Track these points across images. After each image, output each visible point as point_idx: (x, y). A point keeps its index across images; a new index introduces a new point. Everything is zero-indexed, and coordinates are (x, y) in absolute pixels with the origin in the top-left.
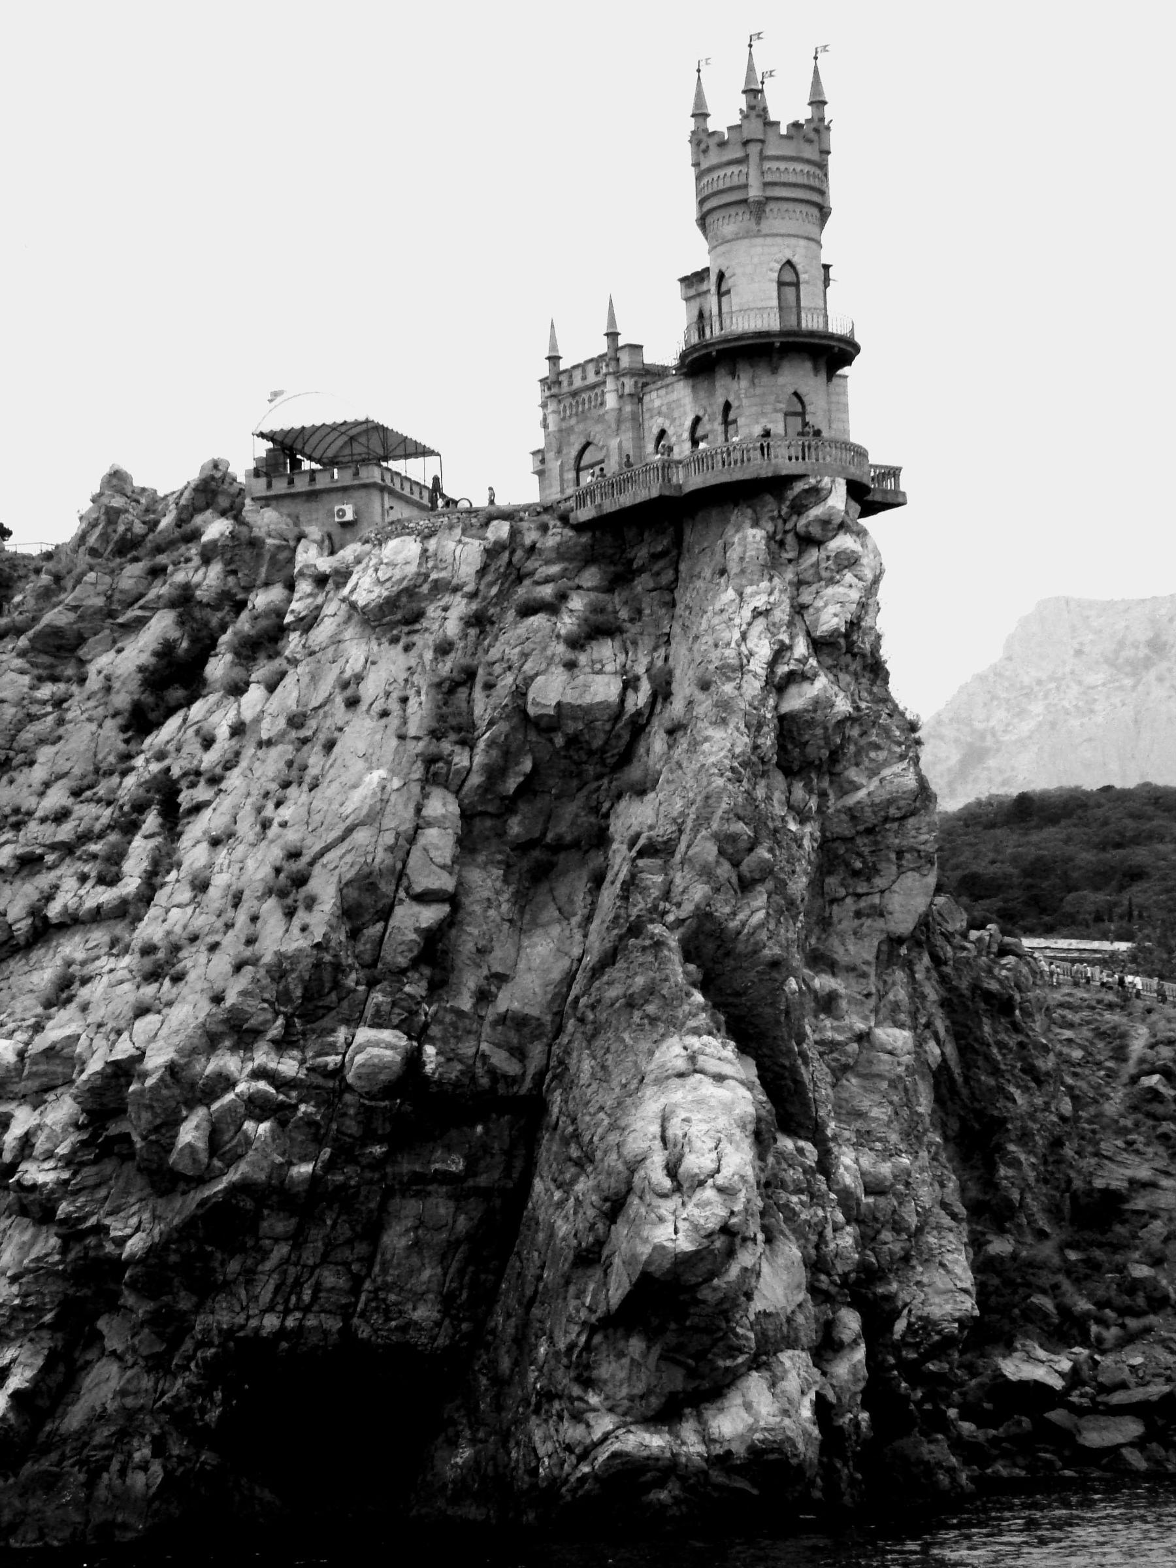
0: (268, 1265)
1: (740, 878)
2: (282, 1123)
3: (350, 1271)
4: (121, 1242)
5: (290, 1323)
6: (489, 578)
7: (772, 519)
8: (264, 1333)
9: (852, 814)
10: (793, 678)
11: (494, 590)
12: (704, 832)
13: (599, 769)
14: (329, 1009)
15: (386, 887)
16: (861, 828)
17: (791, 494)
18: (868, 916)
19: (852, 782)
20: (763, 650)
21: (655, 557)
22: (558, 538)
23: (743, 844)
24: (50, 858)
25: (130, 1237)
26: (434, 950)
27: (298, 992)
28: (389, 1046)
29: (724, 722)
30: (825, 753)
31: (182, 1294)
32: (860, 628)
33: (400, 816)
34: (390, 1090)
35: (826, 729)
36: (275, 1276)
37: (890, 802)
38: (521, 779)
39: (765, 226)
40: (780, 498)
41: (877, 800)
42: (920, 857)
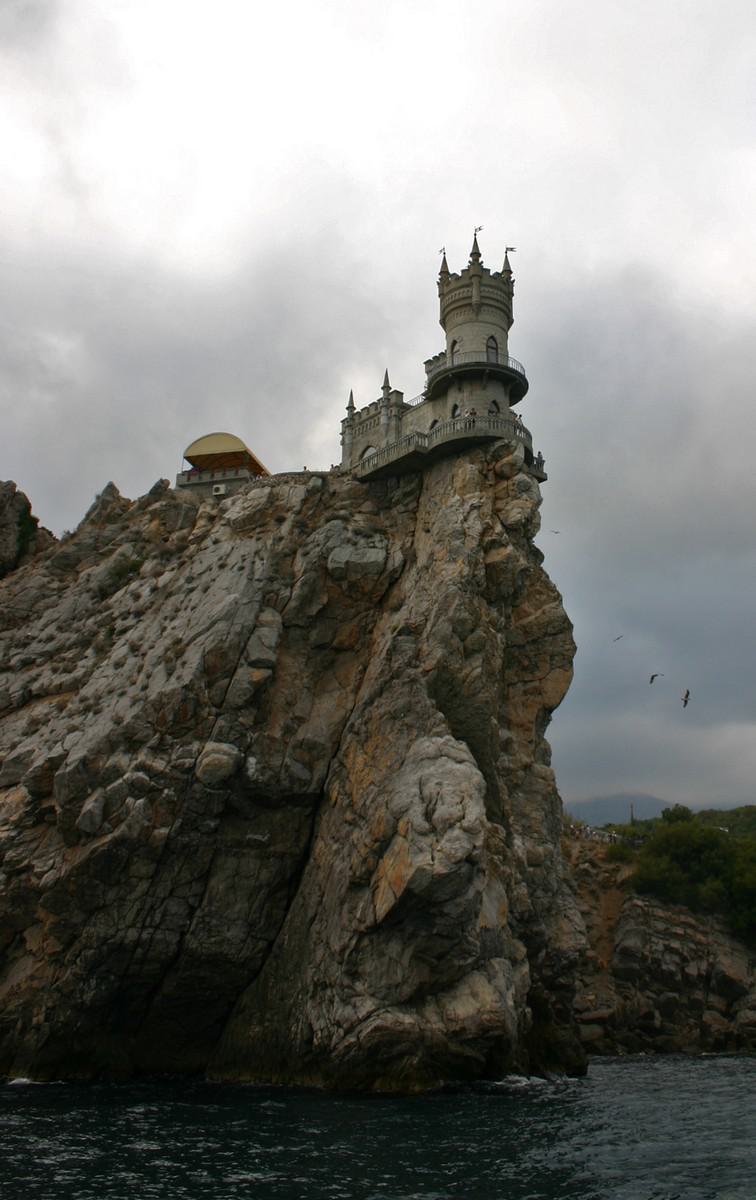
0: (133, 896)
1: (465, 648)
2: (151, 801)
3: (188, 902)
4: (40, 876)
5: (145, 936)
6: (308, 505)
7: (481, 462)
8: (127, 941)
9: (526, 630)
10: (495, 544)
11: (311, 512)
12: (443, 618)
13: (368, 604)
14: (189, 729)
15: (232, 656)
16: (530, 639)
17: (492, 449)
18: (531, 694)
19: (525, 612)
20: (478, 527)
21: (406, 495)
23: (469, 626)
24: (39, 661)
25: (46, 872)
26: (258, 697)
27: (171, 718)
28: (225, 753)
29: (454, 561)
30: (512, 590)
31: (76, 912)
32: (531, 523)
33: (246, 617)
34: (225, 783)
35: (513, 574)
36: (137, 903)
37: (549, 623)
38: (321, 607)
39: (480, 318)
40: (486, 452)
41: (542, 622)
42: (564, 659)
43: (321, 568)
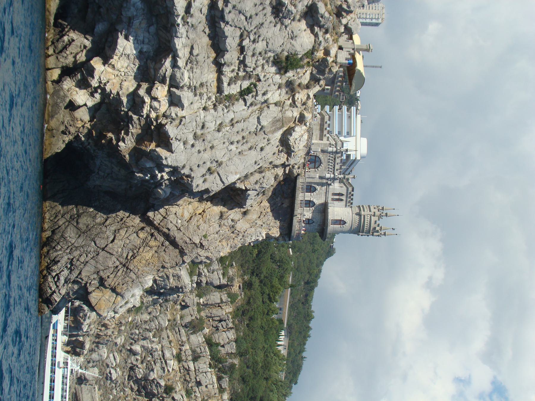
22: (295, 173)
25: (125, 143)
43: (247, 190)
